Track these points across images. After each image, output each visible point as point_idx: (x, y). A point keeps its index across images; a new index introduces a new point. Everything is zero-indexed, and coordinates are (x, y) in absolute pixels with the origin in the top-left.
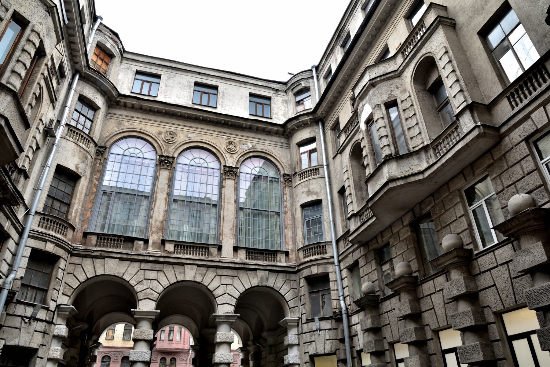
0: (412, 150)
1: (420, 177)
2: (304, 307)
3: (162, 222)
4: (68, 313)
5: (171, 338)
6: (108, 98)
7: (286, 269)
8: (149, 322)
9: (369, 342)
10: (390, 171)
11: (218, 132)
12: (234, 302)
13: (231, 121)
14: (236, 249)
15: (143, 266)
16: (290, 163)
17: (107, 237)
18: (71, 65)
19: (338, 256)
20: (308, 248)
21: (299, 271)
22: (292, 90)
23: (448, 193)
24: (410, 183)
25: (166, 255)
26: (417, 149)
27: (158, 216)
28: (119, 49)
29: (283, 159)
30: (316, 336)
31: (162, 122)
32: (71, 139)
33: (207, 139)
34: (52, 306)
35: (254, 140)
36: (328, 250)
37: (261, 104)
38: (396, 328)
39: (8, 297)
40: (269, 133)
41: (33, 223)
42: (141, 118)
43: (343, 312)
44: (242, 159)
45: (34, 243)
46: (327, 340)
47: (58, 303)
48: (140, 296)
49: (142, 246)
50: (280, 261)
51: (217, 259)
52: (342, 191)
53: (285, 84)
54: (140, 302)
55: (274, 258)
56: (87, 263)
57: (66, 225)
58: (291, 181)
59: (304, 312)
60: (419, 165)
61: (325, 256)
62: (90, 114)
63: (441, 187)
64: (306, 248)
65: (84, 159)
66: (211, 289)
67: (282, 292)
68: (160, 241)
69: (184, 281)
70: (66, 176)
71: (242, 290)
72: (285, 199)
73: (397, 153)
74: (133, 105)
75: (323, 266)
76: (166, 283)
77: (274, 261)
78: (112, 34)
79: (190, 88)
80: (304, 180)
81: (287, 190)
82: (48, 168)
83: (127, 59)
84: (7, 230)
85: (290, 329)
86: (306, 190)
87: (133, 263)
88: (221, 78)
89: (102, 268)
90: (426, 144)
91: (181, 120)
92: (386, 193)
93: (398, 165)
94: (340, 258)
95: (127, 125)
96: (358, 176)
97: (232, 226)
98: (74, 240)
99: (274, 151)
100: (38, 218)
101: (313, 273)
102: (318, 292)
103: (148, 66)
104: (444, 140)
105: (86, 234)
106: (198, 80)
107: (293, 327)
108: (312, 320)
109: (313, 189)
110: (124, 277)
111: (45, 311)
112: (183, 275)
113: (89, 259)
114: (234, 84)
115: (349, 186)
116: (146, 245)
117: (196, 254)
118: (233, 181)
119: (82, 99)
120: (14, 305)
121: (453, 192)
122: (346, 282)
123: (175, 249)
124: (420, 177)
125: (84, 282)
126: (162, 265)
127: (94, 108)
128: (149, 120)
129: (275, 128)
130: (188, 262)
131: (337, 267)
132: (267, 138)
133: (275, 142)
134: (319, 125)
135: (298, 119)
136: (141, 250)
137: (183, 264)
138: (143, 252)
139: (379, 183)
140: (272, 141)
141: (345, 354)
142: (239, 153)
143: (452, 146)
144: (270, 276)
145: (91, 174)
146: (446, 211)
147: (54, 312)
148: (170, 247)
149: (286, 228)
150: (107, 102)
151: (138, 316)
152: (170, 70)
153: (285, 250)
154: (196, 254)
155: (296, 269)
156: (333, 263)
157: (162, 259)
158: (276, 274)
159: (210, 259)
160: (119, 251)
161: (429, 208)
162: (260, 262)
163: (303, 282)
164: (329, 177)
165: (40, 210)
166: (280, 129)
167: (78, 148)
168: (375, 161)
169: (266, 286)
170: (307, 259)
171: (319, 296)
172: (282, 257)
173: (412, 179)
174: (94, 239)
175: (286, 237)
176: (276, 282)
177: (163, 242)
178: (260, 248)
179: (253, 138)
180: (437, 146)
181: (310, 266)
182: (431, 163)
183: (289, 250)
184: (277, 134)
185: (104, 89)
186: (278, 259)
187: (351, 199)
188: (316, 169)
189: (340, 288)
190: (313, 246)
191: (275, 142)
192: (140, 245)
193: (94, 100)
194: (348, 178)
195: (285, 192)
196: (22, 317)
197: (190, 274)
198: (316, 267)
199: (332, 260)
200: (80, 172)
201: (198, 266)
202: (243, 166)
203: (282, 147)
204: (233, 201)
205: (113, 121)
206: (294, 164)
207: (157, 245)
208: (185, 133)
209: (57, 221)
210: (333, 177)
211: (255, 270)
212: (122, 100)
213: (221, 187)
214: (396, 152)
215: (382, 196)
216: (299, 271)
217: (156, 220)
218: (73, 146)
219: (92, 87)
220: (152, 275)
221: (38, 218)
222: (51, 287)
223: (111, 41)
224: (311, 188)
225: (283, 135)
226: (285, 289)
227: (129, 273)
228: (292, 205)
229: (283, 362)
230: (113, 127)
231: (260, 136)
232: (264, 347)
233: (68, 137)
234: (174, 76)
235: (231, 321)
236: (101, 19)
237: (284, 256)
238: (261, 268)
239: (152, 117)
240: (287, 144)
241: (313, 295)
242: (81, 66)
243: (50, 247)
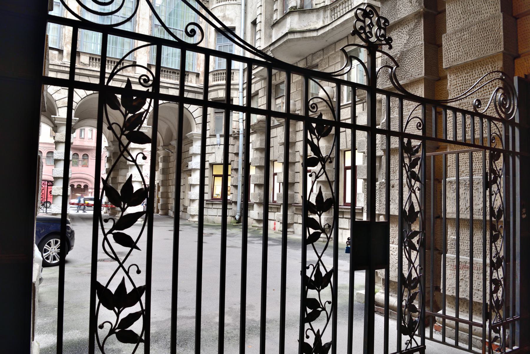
0: (315, 7)
1: (314, 34)
7: (196, 90)
9: (255, 158)
10: (294, 22)
20: (217, 72)
23: (333, 52)
24: (305, 38)
25: (82, 67)
26: (318, 6)
30: (216, 149)
38: (277, 151)
43: (241, 132)
49: (57, 56)
50: (191, 82)
52: (254, 23)
54: (59, 109)
60: (315, 22)
63: (331, 45)
64: (215, 73)
73: (302, 7)
80: (221, 4)
85: (195, 142)
90: (326, 4)
92: (284, 42)
93: (299, 18)
96: (270, 13)
104: (340, 5)
108: (215, 136)
109: (228, 15)
115: (260, 22)
116: (60, 55)
121: (337, 52)
123: (90, 62)
124: (314, 34)
131: (241, 94)
136: (56, 60)
139: (281, 31)
141: (238, 165)
143: (342, 15)
146: (329, 66)
151: (58, 122)
153: (196, 71)
161: (318, 60)
164: (246, 5)
168: (283, 8)
173: (308, 35)
178: (173, 68)
180: (334, 8)
182: (326, 24)
186: (189, 79)
187: (260, 35)
190: (222, 72)
192: (55, 54)
194: (261, 14)
199: (237, 87)
204: (148, 18)
210: (249, 5)
214: (301, 5)
215: (281, 45)
224: (226, 14)
229: (188, 166)
232: (172, 152)
237: (195, 77)
238: (173, 86)
241: (218, 115)
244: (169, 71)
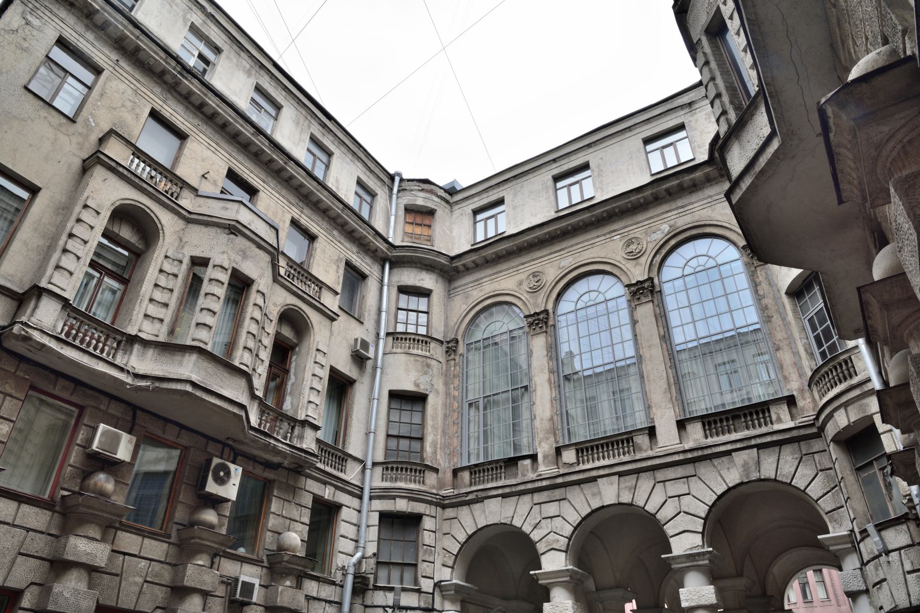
3: (552, 419)
4: (453, 592)
5: (809, 598)
6: (441, 270)
7: (795, 433)
8: (566, 588)
11: (605, 235)
12: (699, 525)
13: (618, 207)
14: (681, 425)
15: (538, 497)
17: (481, 469)
18: (372, 257)
25: (566, 471)
27: (543, 411)
28: (439, 197)
30: (885, 566)
31: (518, 266)
32: (399, 350)
33: (591, 256)
34: (427, 585)
35: (670, 214)
36: (858, 365)
37: (671, 144)
39: (354, 583)
40: (695, 187)
41: (376, 480)
42: (491, 275)
44: (659, 258)
45: (379, 505)
46: (909, 572)
47: (436, 580)
48: (541, 548)
49: (529, 467)
50: (779, 420)
51: (650, 453)
55: (764, 418)
56: (464, 513)
57: (422, 469)
61: (855, 380)
62: (422, 304)
64: (817, 378)
65: (426, 369)
66: (653, 511)
67: (800, 482)
68: (553, 451)
69: (603, 507)
70: (409, 400)
71: (710, 498)
74: (474, 262)
75: (856, 405)
76: (575, 519)
77: (766, 424)
78: (421, 185)
79: (547, 192)
82: (376, 401)
83: (457, 203)
84: (331, 498)
87: (522, 497)
88: (589, 146)
89: (483, 517)
91: (545, 247)
95: (477, 294)
97: (666, 386)
98: (441, 485)
99: (713, 215)
100: (379, 470)
101: (842, 426)
102: (871, 463)
103: (484, 196)
105: (455, 472)
106: (556, 172)
107: (847, 552)
110: (514, 523)
111: (416, 595)
112: (598, 498)
113: (465, 507)
114: (614, 141)
117: (614, 456)
118: (651, 304)
119: (404, 290)
120: (371, 592)
125: (465, 542)
126: (563, 490)
127: (425, 293)
128: (501, 272)
129: (698, 174)
130: (602, 472)
132: (694, 198)
133: (710, 197)
137: (594, 479)
138: (532, 476)
140: (703, 199)
142: (649, 251)
144: (762, 457)
145: (446, 384)
147: (433, 594)
148: (569, 456)
149: (778, 349)
150: (443, 277)
152: (514, 182)
153: (786, 394)
154: (614, 456)
157: (560, 480)
158: (777, 449)
159: (638, 456)
160: (500, 483)
162: (734, 436)
163: (834, 452)
165: (380, 458)
166: (708, 169)
167: (412, 358)
170: (825, 400)
171: (875, 473)
174: (466, 475)
177: (558, 451)
179: (668, 212)
183: (795, 393)
185: (427, 263)
186: (774, 417)
191: (710, 197)
193: (419, 284)
196: (384, 607)
197: (609, 493)
200: (422, 389)
201: (620, 474)
202: (665, 270)
205: (458, 298)
207: (550, 458)
208: (553, 265)
209: (404, 466)
211: (728, 453)
212: (458, 264)
213: (634, 323)
217: (542, 419)
218: (403, 358)
219: (410, 269)
220: (551, 509)
221: (379, 470)
222: (421, 558)
223: (422, 194)
226: (804, 476)
227: (518, 513)
230: (461, 306)
231: (680, 203)
233: (395, 350)
234: (522, 187)
235: (701, 563)
236: (399, 174)
237: (785, 407)
238: (738, 445)
239: (504, 266)
242: (383, 252)
243: (402, 505)
244: (723, 417)
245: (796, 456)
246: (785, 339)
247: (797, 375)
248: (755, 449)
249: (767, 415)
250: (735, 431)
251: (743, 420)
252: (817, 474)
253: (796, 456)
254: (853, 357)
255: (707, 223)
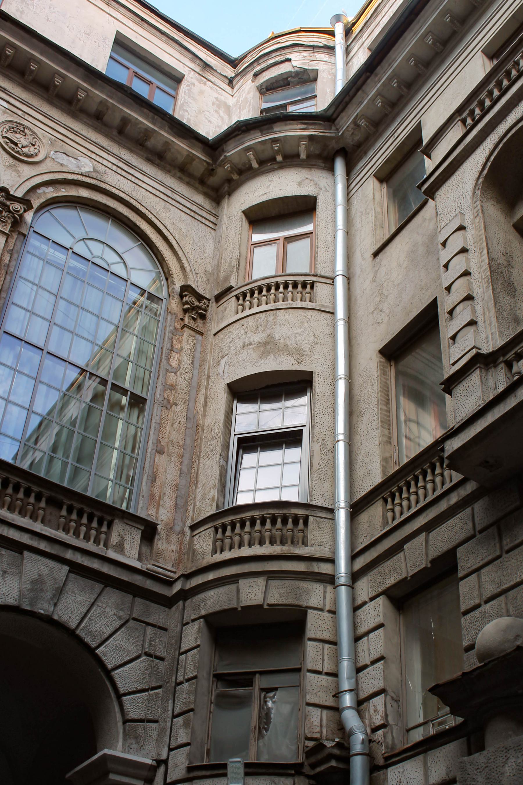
2: (186, 724)
7: (137, 580)
13: (38, 62)
16: (209, 268)
19: (353, 557)
21: (185, 595)
22: (256, 75)
29: (187, 248)
44: (50, 193)
53: (233, 63)
55: (99, 533)
58: (203, 317)
59: (182, 737)
64: (227, 520)
67: (109, 654)
72: (174, 363)
77: (97, 542)
81: (187, 339)
86: (260, 337)
94: (360, 563)
122: (375, 645)
134: (331, 169)
135: (270, 130)
142: (42, 168)
144: (70, 586)
149: (160, 452)
155: (177, 587)
156: (330, 580)
158: (98, 587)
163: (193, 635)
169: (48, 620)
172: (132, 539)
175: (154, 479)
176: (92, 616)
181: (234, 579)
184: (182, 170)
186: (114, 539)
188: (304, 285)
189: (346, 666)
190: (256, 513)
195: (177, 346)
198: (261, 581)
199: (325, 568)
203: (193, 215)
206: (224, 267)
216: (185, 595)
224: (277, 335)
225: (202, 181)
228: (194, 388)
237: (137, 536)
238: (43, 546)
240: (211, 213)
244: (35, 488)
245: (121, 613)
246: (178, 444)
247: (173, 503)
248: (66, 568)
249: (104, 529)
250: (43, 522)
251: (64, 513)
252: (138, 657)
253: (121, 613)
254: (311, 519)
255: (150, 216)
